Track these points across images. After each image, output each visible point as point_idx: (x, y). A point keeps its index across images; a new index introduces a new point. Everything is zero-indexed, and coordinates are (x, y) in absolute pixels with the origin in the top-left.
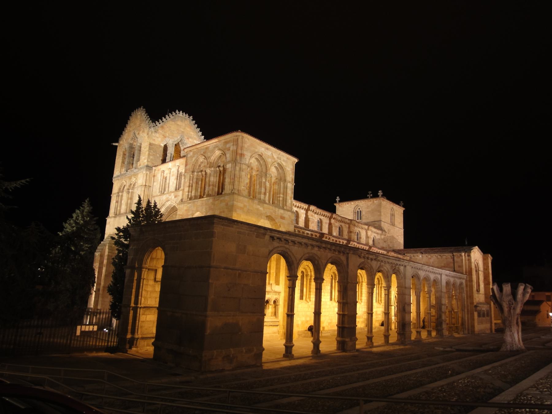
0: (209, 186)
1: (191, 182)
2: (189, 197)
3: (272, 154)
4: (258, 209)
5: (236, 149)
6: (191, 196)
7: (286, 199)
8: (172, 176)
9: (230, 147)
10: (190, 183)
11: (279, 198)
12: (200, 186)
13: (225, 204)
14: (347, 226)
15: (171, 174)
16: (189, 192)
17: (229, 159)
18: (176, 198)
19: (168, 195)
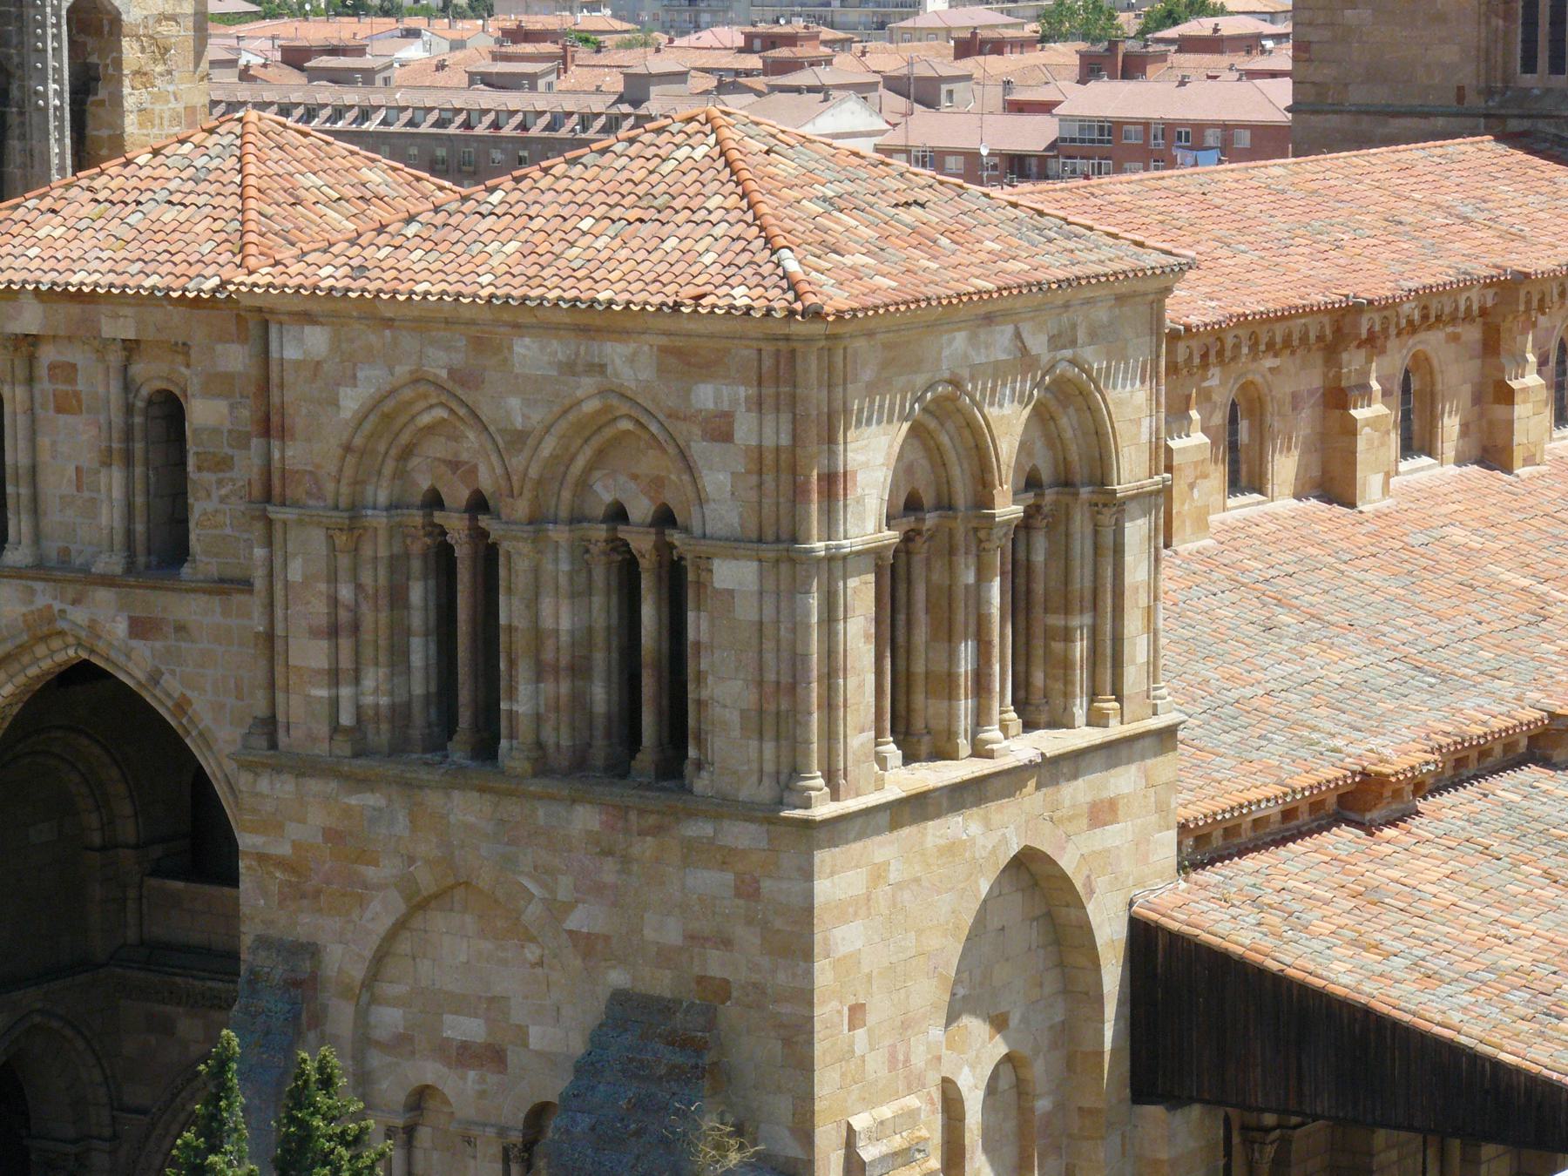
0: (539, 677)
1: (346, 593)
2: (346, 719)
3: (1018, 335)
4: (951, 849)
5: (785, 440)
6: (359, 708)
7: (1118, 640)
8: (59, 410)
9: (727, 416)
10: (334, 601)
11: (1057, 646)
12: (417, 620)
13: (729, 877)
14: (1472, 333)
15: (45, 386)
16: (334, 676)
17: (736, 521)
18: (158, 645)
19: (45, 596)
